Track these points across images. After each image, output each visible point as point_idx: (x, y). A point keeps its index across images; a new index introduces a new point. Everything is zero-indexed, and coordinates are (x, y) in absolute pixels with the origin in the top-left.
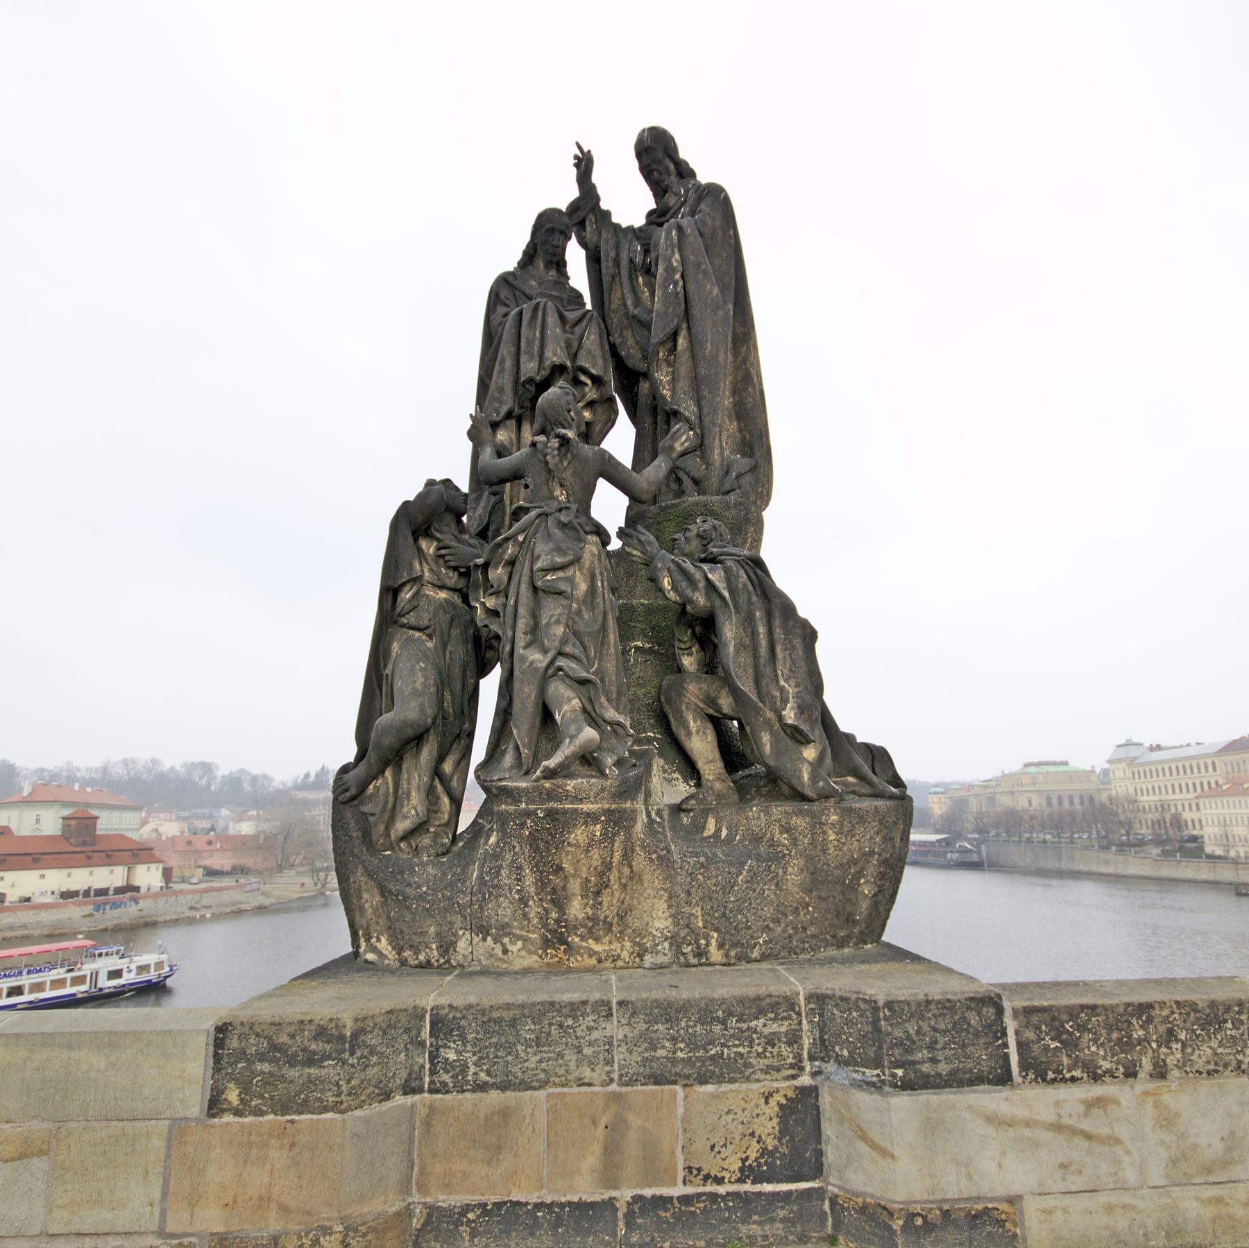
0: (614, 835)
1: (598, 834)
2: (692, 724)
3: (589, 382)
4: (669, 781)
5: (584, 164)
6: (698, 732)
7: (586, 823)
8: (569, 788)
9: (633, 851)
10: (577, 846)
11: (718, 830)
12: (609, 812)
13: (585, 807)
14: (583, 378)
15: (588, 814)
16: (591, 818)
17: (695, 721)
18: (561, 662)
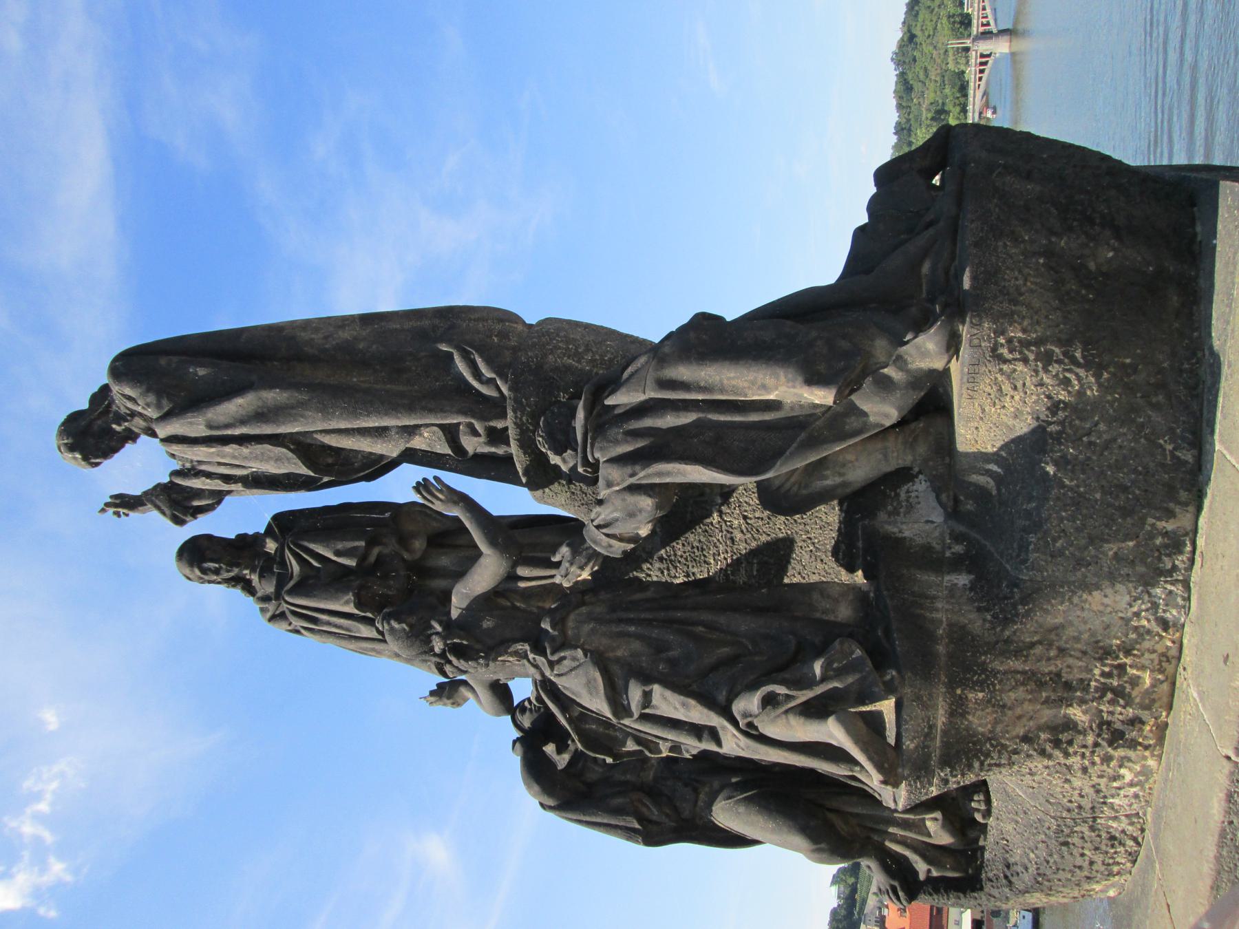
0: (984, 670)
1: (980, 695)
2: (829, 482)
3: (376, 551)
4: (910, 507)
5: (125, 503)
6: (841, 475)
7: (963, 715)
8: (912, 746)
9: (1007, 641)
10: (996, 722)
11: (989, 473)
12: (951, 686)
13: (941, 719)
14: (372, 559)
15: (952, 714)
16: (958, 709)
17: (826, 478)
18: (738, 707)
